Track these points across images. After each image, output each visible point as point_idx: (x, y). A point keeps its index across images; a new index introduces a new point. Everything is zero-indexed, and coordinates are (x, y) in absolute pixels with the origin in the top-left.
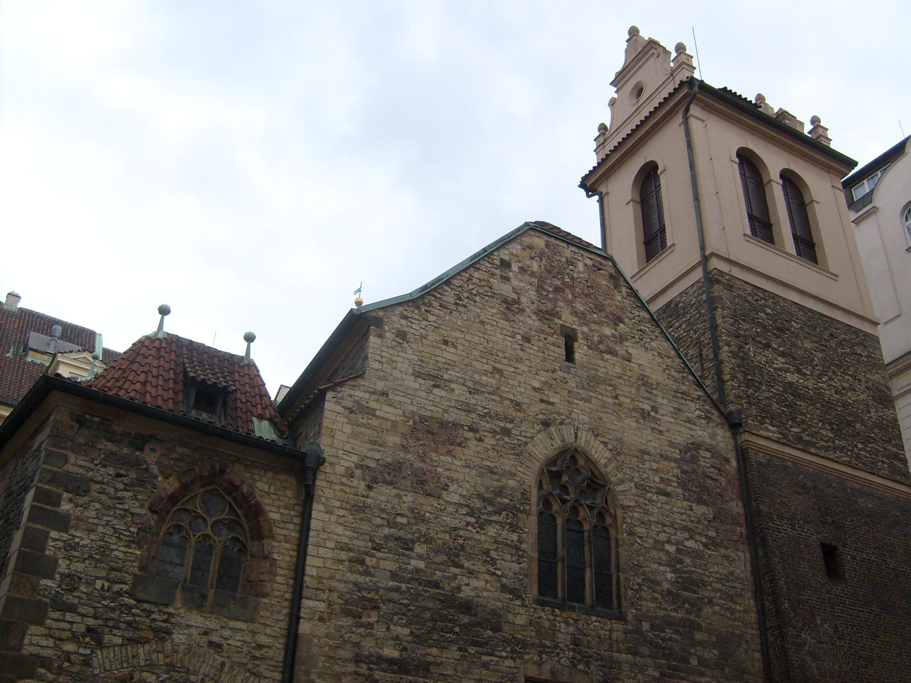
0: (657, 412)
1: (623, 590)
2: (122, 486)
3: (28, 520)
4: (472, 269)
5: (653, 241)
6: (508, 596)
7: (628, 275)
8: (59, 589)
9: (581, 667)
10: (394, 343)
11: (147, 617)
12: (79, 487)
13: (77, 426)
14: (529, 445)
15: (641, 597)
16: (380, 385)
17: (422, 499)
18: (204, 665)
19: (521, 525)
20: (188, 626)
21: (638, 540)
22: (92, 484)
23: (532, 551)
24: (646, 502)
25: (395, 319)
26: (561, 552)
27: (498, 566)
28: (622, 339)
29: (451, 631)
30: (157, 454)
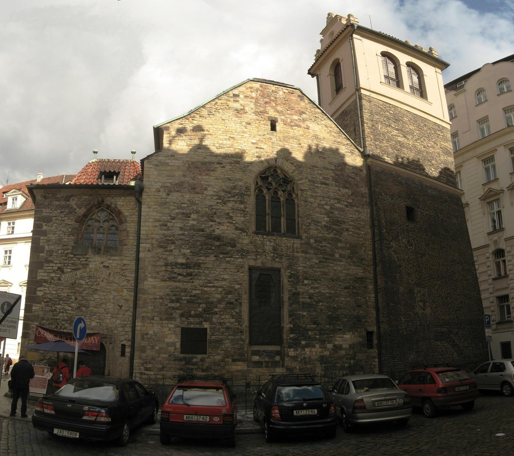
6: (239, 232)
9: (277, 260)
29: (211, 249)
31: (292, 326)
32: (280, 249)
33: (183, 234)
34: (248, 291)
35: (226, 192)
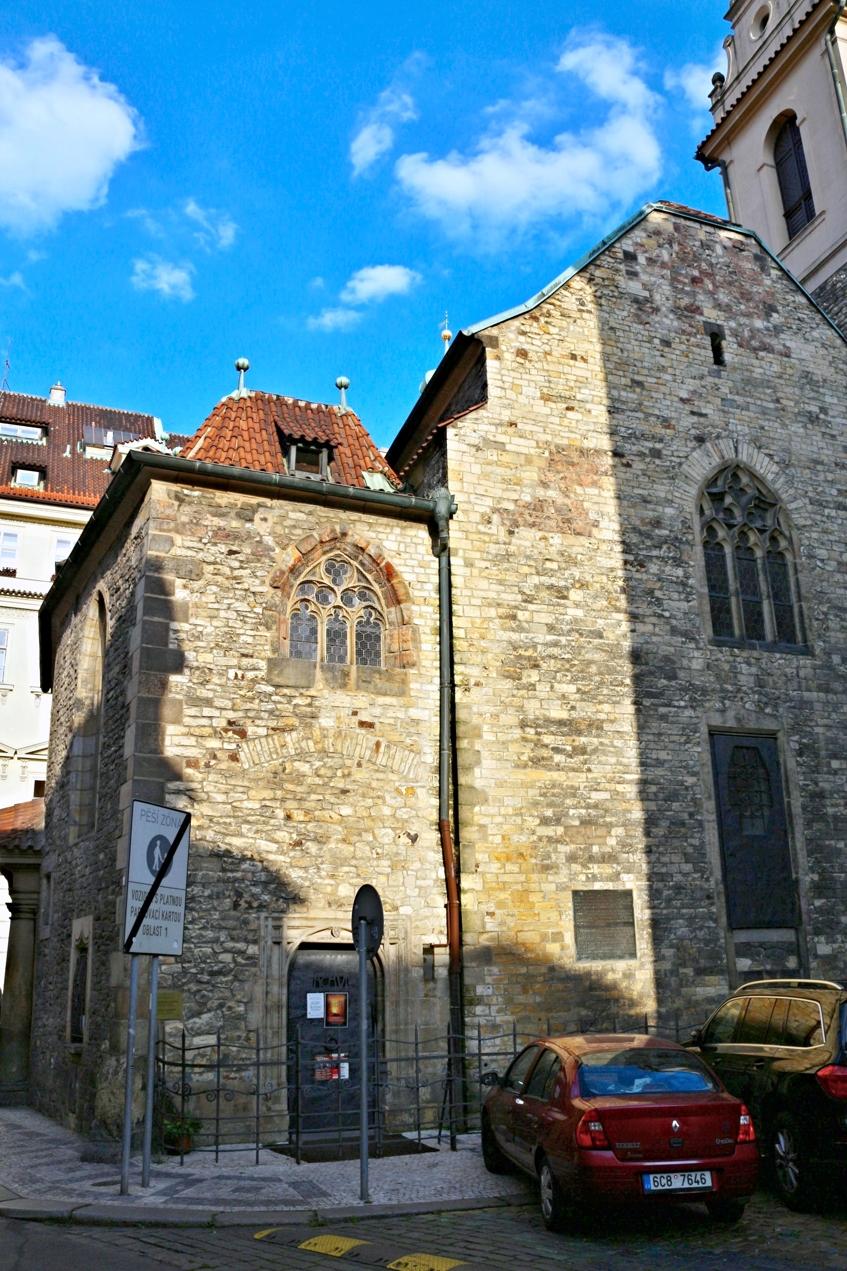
0: (826, 414)
1: (807, 621)
2: (236, 564)
3: (144, 614)
4: (592, 267)
5: (798, 211)
7: (774, 251)
8: (190, 684)
10: (515, 365)
11: (289, 702)
13: (176, 503)
14: (684, 466)
15: (828, 627)
16: (506, 416)
17: (572, 539)
19: (685, 558)
21: (819, 563)
22: (204, 565)
23: (701, 586)
24: (824, 519)
25: (512, 336)
26: (733, 584)
27: (665, 607)
28: (777, 330)
30: (270, 523)
31: (816, 877)
32: (771, 683)
33: (556, 644)
34: (712, 789)
35: (641, 533)
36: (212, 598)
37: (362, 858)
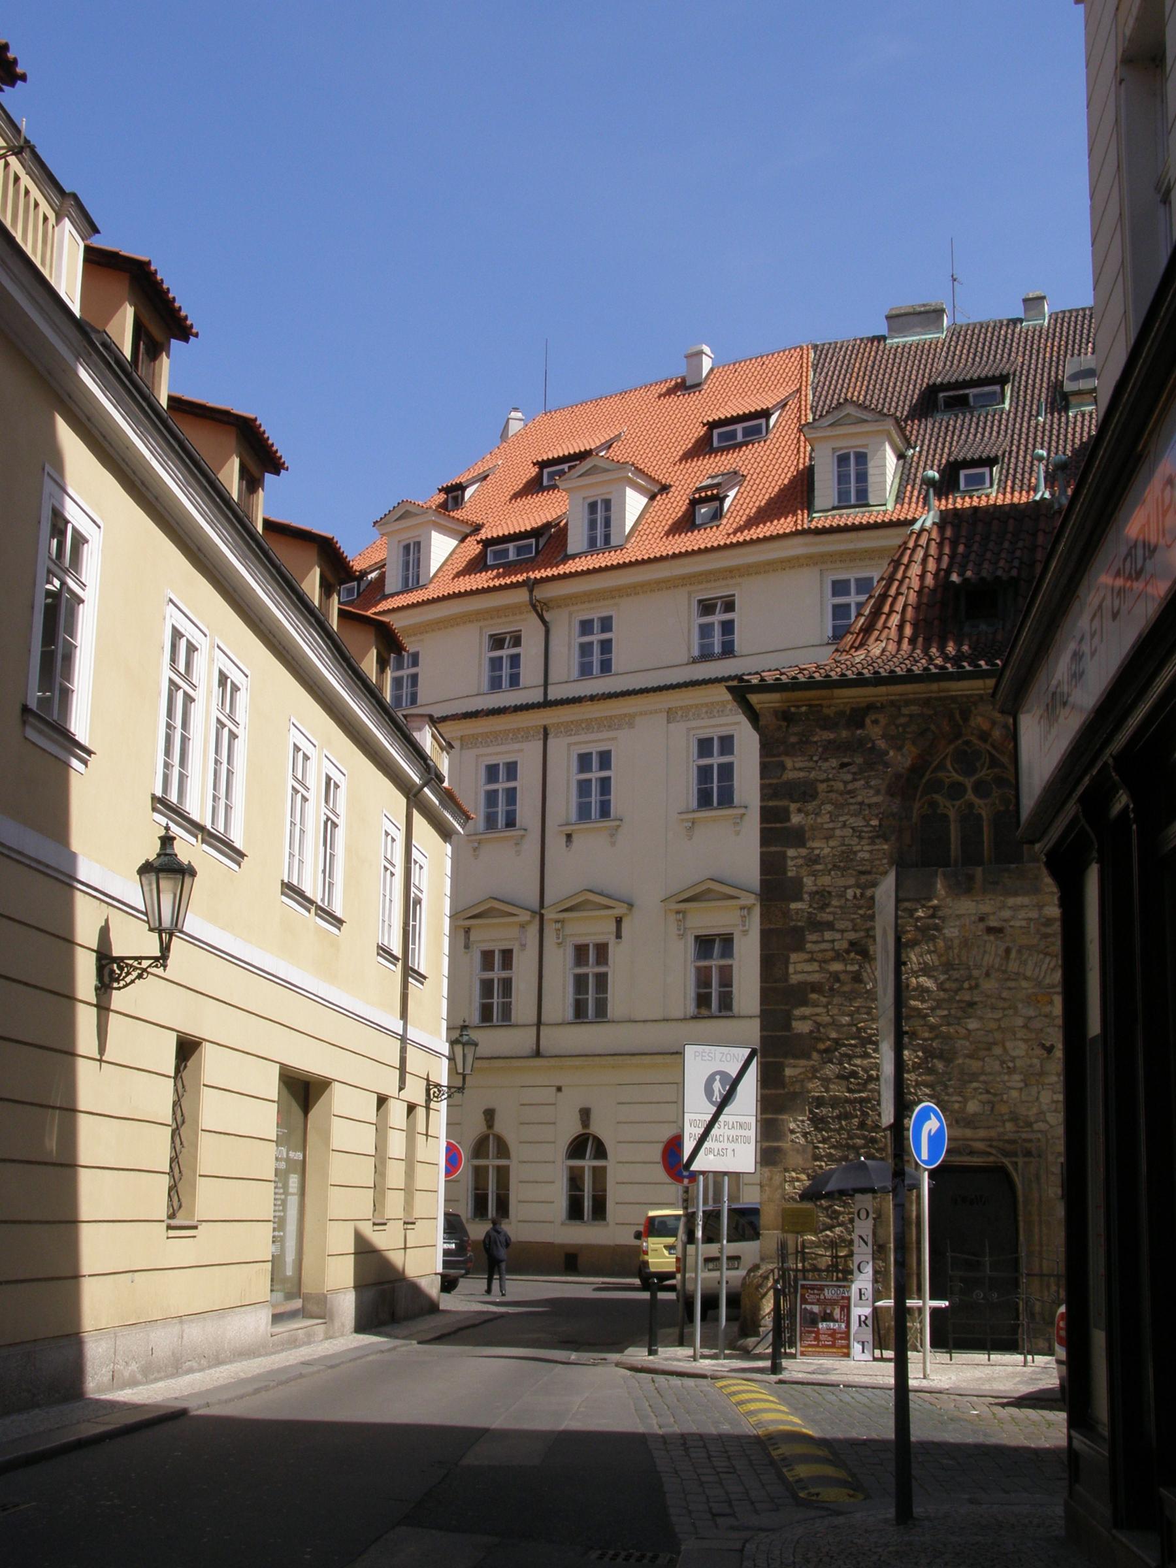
2: (849, 777)
12: (804, 792)
18: (986, 958)
20: (959, 916)
36: (827, 818)
37: (990, 1074)
